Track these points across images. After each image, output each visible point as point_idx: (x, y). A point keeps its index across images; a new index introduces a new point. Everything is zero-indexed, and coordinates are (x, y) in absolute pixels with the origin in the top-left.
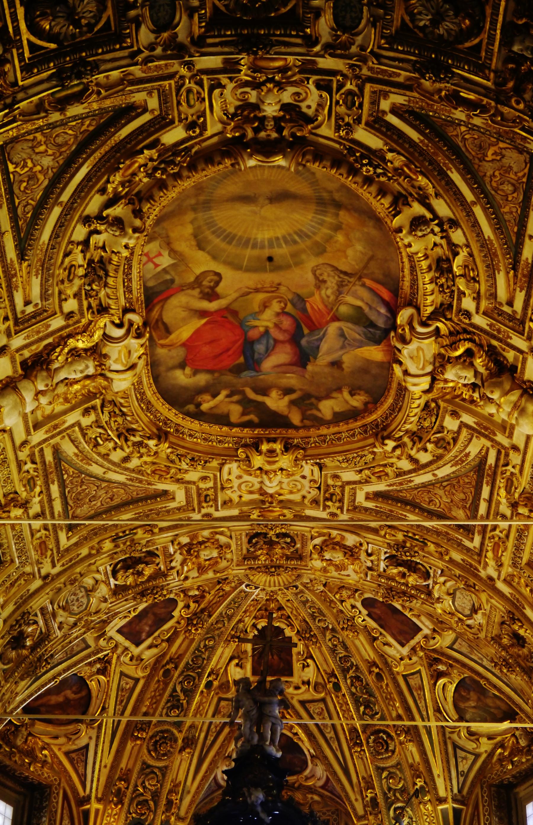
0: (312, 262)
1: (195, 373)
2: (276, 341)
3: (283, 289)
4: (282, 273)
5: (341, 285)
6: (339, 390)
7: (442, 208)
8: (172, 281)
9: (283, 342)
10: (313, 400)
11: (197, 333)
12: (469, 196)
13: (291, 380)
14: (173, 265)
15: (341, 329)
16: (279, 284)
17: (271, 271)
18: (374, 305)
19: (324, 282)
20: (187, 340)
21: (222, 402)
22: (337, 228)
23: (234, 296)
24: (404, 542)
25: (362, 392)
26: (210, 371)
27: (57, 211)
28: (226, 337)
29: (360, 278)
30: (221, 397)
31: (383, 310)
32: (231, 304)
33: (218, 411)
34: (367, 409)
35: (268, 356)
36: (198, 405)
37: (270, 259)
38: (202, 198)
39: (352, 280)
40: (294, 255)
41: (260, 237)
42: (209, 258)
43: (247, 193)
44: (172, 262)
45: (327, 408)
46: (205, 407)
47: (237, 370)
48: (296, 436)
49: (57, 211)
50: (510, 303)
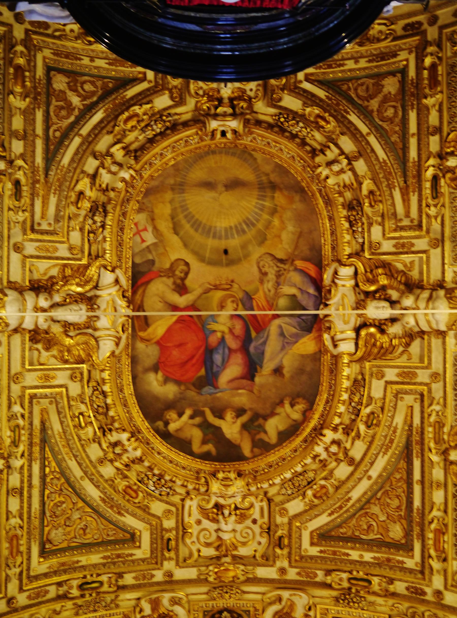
0: (257, 252)
1: (166, 381)
2: (230, 350)
3: (235, 286)
4: (234, 268)
5: (278, 275)
6: (281, 403)
7: (347, 144)
8: (152, 262)
9: (235, 351)
10: (261, 421)
11: (169, 330)
12: (364, 129)
13: (242, 398)
14: (155, 244)
15: (280, 327)
16: (232, 281)
17: (228, 265)
18: (304, 289)
19: (266, 274)
20: (162, 338)
21: (186, 423)
22: (274, 212)
23: (199, 291)
24: (350, 589)
25: (300, 400)
26: (178, 382)
27: (77, 141)
28: (192, 341)
29: (292, 264)
30: (185, 417)
31: (312, 291)
32: (195, 301)
33: (183, 435)
34: (306, 415)
35: (224, 369)
36: (167, 424)
37: (226, 252)
38: (178, 179)
39: (286, 267)
40: (244, 246)
41: (218, 224)
42: (181, 244)
43: (210, 180)
44: (155, 241)
45: (273, 426)
46: (172, 427)
47: (200, 385)
48: (246, 467)
49: (77, 141)
50: (407, 215)
